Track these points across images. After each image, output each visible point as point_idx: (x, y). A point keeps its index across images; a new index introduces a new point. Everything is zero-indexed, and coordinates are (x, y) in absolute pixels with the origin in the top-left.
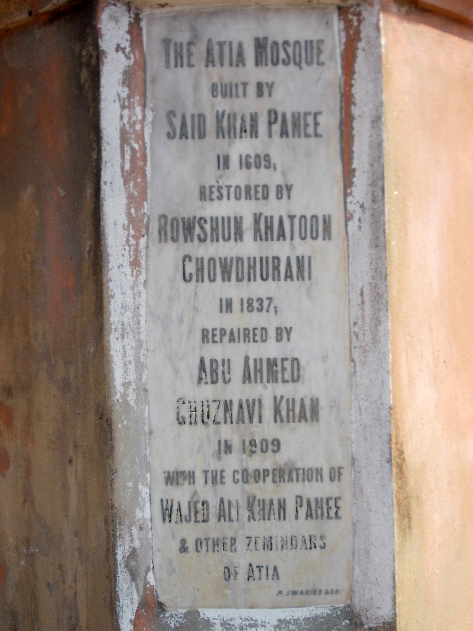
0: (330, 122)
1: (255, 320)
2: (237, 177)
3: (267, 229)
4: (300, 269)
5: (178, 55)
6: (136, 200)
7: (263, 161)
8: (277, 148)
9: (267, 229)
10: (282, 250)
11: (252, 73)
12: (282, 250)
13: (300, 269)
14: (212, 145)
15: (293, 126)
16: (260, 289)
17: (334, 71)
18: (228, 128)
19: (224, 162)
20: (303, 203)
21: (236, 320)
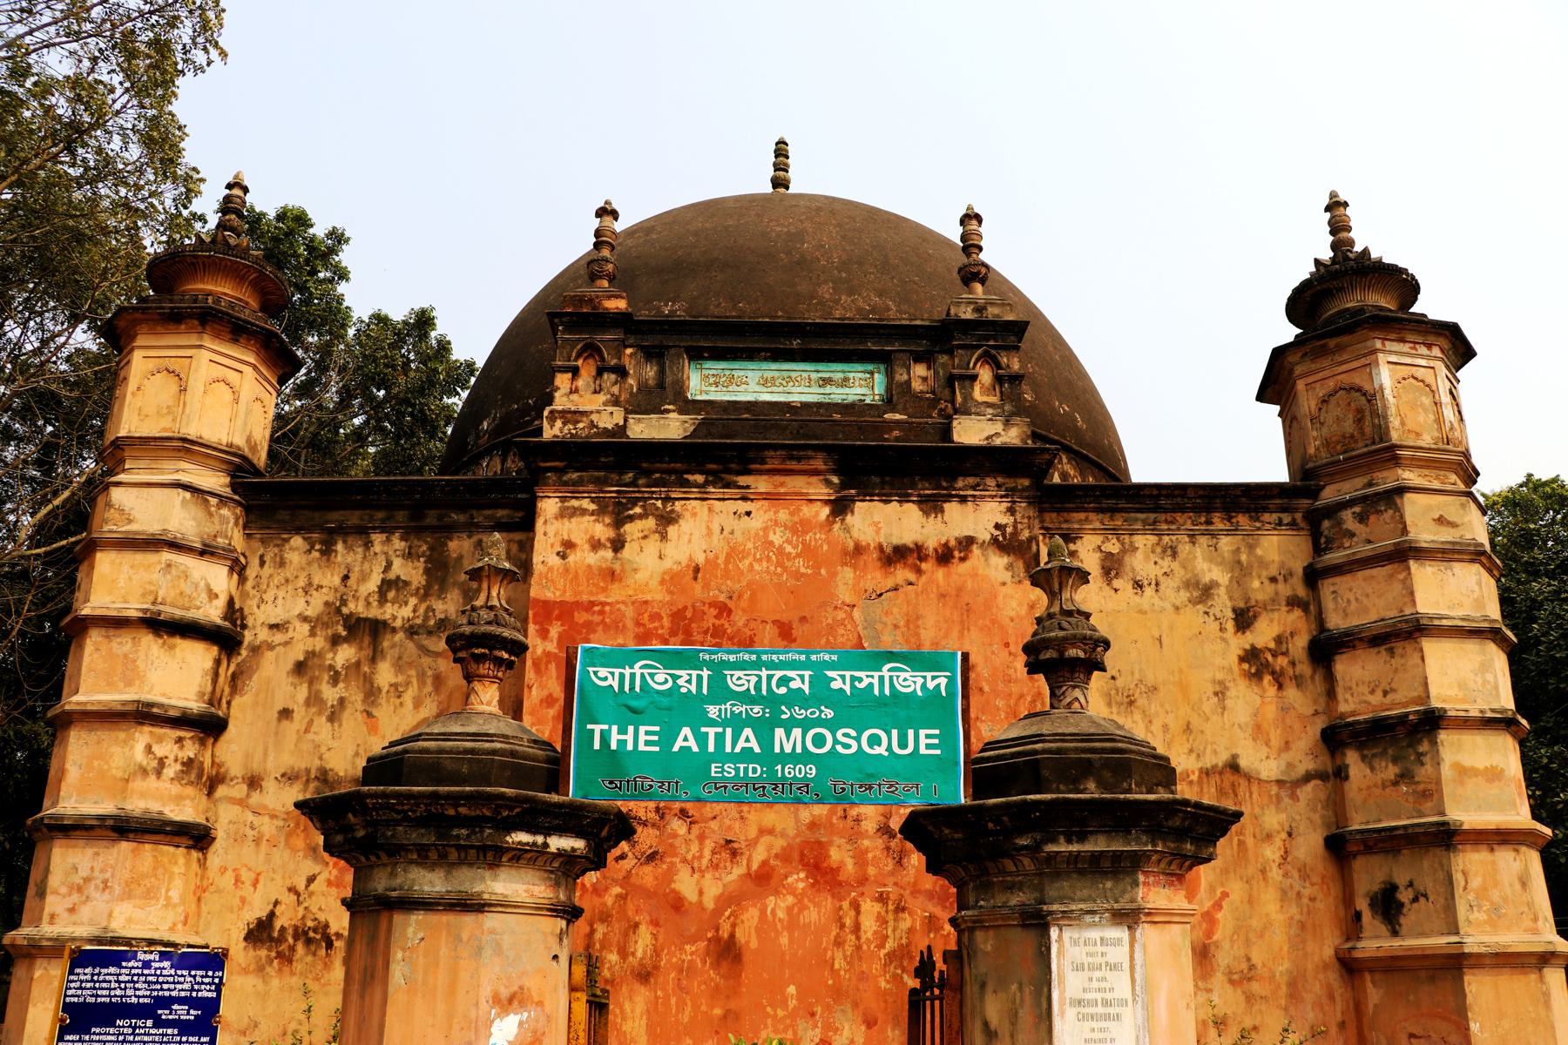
0: (1126, 966)
1: (1101, 1035)
2: (1095, 984)
3: (1106, 1003)
4: (1118, 1017)
5: (1075, 943)
6: (1062, 993)
7: (1104, 979)
8: (1108, 975)
9: (1106, 1003)
10: (1111, 1010)
11: (1100, 949)
12: (1111, 1010)
13: (1118, 1017)
14: (1087, 974)
15: (1114, 967)
16: (1104, 1024)
17: (1127, 948)
18: (1092, 968)
19: (1091, 979)
20: (1117, 995)
21: (1096, 1035)
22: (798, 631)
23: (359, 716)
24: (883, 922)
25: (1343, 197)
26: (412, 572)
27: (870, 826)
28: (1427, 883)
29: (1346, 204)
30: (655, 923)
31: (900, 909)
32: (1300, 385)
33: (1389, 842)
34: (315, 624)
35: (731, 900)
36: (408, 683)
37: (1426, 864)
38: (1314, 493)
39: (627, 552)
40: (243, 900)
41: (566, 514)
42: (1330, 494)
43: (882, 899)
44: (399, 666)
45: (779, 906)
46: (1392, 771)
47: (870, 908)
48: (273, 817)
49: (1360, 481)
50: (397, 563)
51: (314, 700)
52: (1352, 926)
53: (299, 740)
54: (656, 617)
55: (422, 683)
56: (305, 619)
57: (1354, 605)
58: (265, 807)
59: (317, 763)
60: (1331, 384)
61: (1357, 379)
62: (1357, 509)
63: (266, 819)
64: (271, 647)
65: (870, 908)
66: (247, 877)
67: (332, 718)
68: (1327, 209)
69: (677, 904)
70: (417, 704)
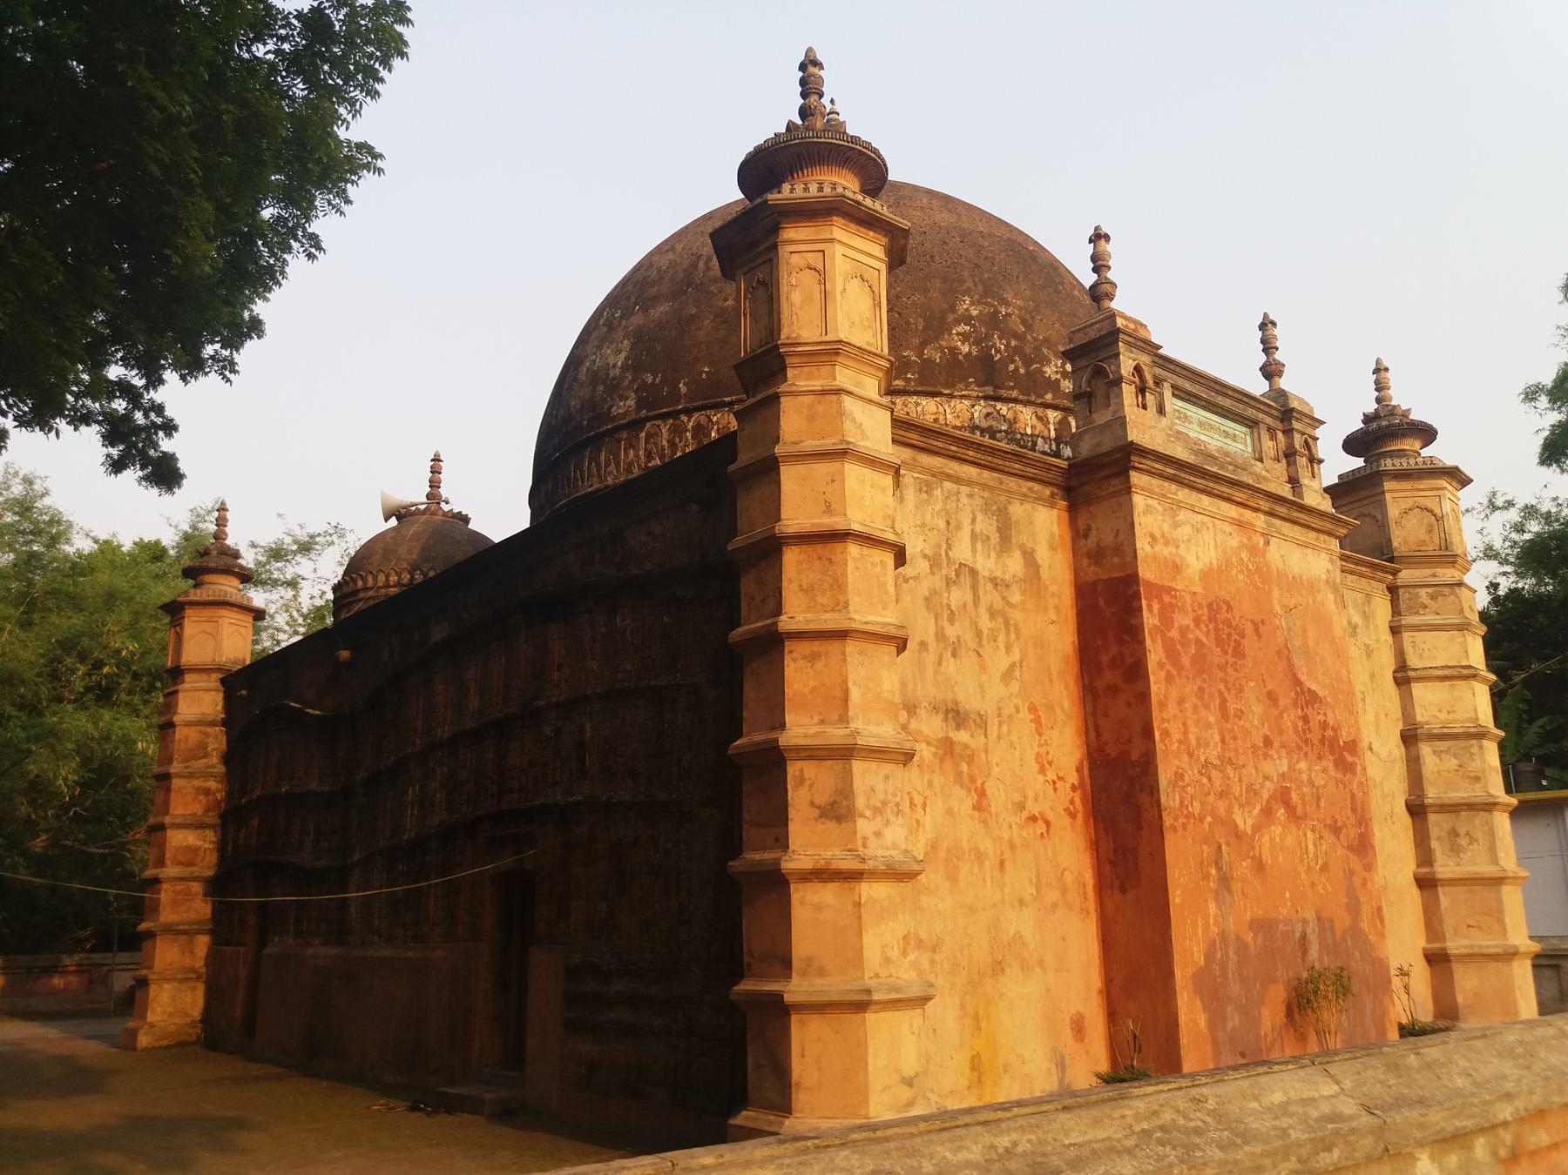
22: (1262, 629)
23: (973, 655)
24: (1315, 845)
25: (1386, 364)
26: (986, 525)
27: (1304, 777)
28: (1478, 834)
29: (1386, 370)
30: (1228, 844)
31: (1321, 837)
32: (1388, 496)
33: (1453, 808)
34: (935, 563)
35: (1257, 828)
36: (998, 630)
37: (1477, 822)
38: (1395, 573)
39: (1182, 550)
40: (918, 822)
41: (1148, 510)
42: (1406, 575)
43: (1313, 830)
44: (993, 614)
45: (1277, 830)
46: (1455, 762)
47: (1309, 834)
48: (929, 744)
49: (1428, 572)
50: (979, 517)
51: (940, 636)
52: (1425, 856)
53: (936, 673)
54: (1200, 605)
55: (1008, 632)
56: (925, 556)
57: (1426, 654)
58: (921, 733)
59: (950, 695)
60: (1410, 503)
61: (1429, 503)
62: (1430, 590)
63: (924, 745)
64: (906, 581)
65: (1309, 834)
66: (918, 800)
67: (954, 655)
68: (1377, 371)
69: (1237, 834)
70: (1008, 649)
